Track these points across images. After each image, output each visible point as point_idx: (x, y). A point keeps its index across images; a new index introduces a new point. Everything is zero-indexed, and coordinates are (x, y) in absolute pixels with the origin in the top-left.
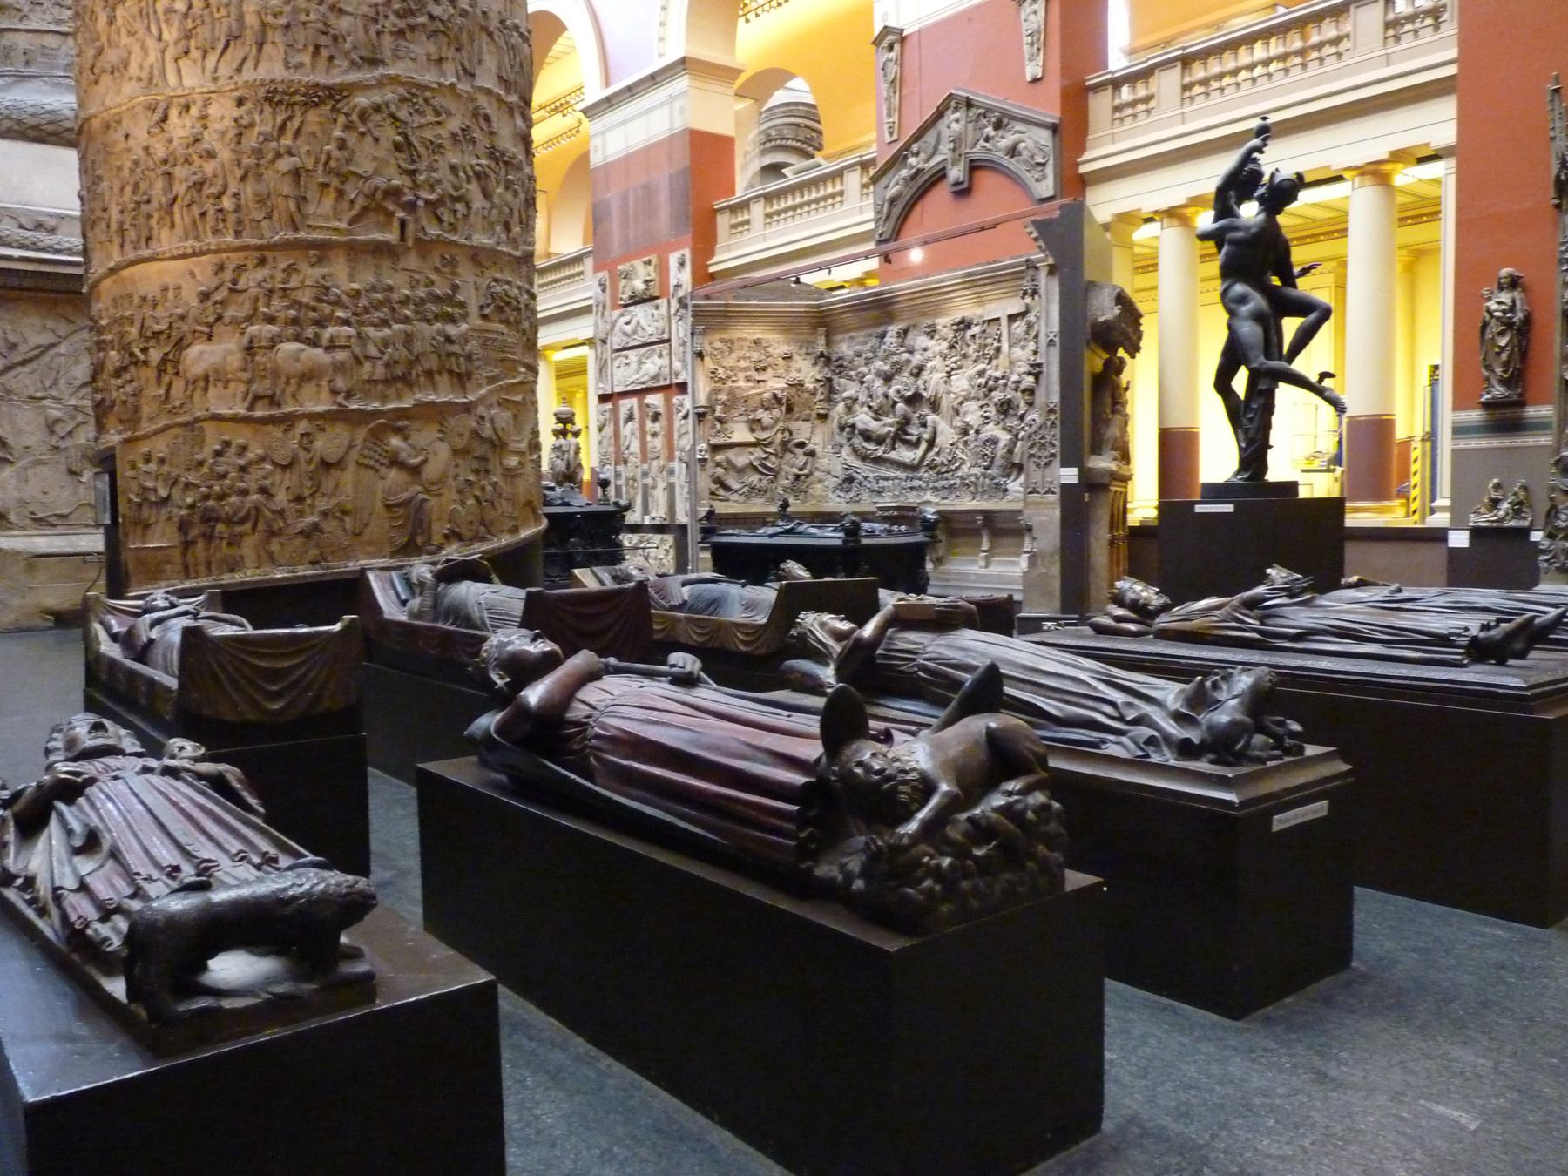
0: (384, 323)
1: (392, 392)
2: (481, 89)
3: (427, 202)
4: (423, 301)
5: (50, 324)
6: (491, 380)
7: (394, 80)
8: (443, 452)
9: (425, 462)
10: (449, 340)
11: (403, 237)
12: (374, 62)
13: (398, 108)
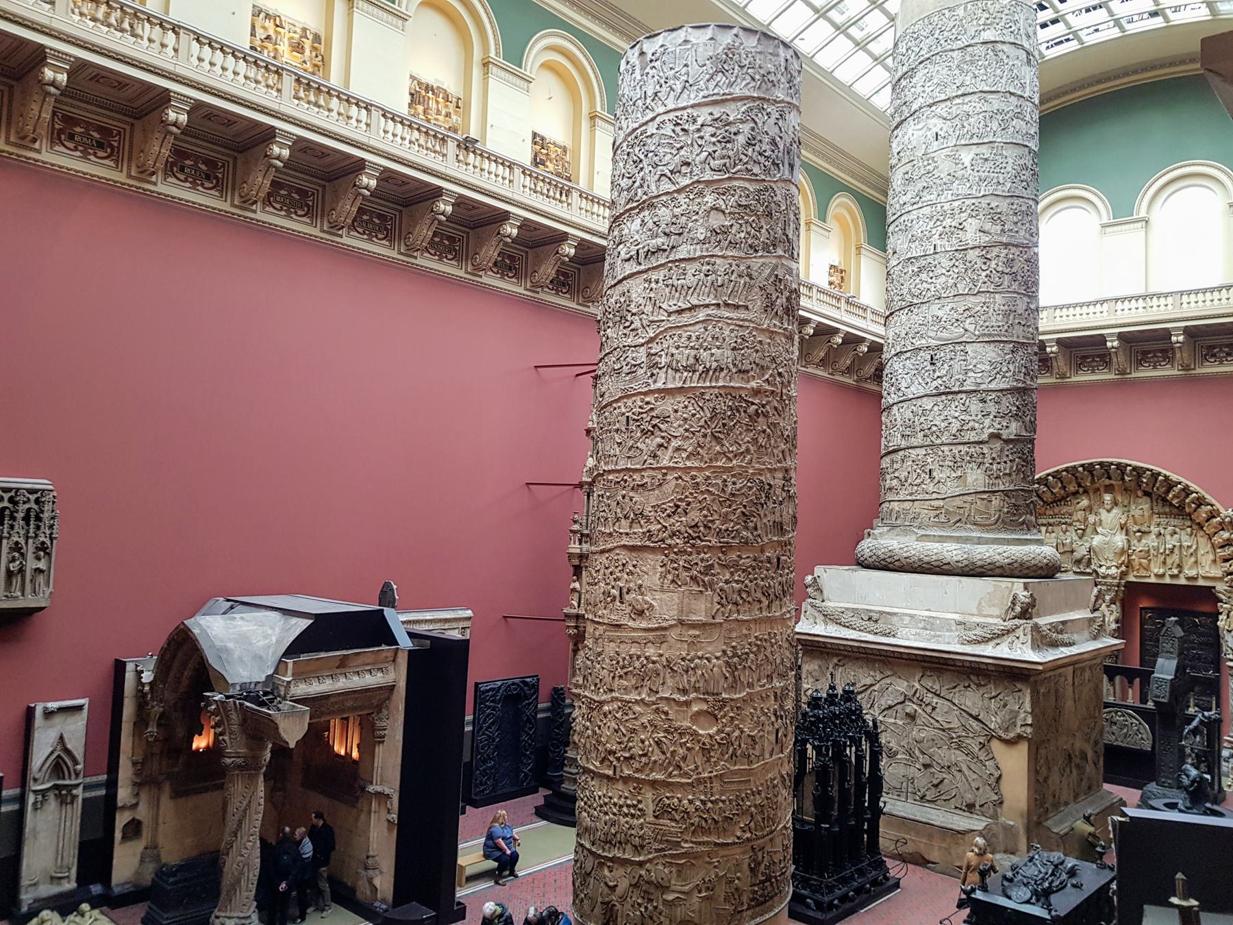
0: (606, 813)
1: (607, 847)
2: (661, 698)
3: (625, 758)
4: (621, 807)
5: (872, 673)
6: (657, 851)
7: (617, 699)
8: (623, 885)
9: (616, 886)
10: (631, 828)
11: (615, 774)
12: (611, 691)
13: (617, 712)
